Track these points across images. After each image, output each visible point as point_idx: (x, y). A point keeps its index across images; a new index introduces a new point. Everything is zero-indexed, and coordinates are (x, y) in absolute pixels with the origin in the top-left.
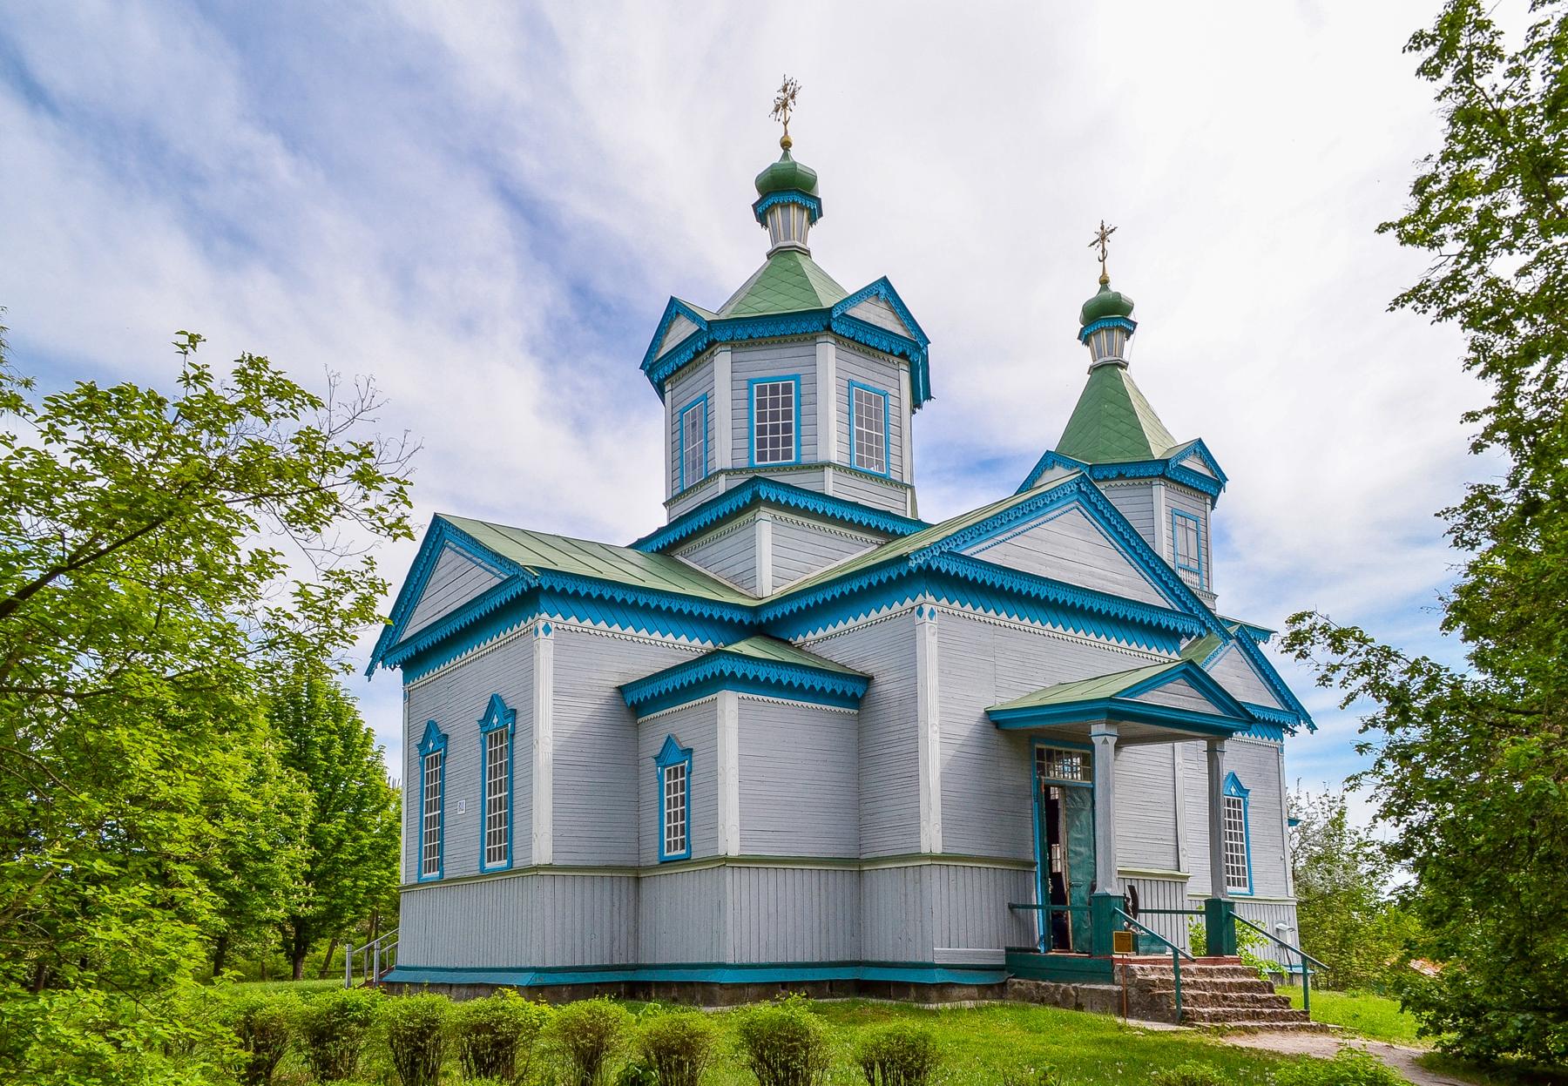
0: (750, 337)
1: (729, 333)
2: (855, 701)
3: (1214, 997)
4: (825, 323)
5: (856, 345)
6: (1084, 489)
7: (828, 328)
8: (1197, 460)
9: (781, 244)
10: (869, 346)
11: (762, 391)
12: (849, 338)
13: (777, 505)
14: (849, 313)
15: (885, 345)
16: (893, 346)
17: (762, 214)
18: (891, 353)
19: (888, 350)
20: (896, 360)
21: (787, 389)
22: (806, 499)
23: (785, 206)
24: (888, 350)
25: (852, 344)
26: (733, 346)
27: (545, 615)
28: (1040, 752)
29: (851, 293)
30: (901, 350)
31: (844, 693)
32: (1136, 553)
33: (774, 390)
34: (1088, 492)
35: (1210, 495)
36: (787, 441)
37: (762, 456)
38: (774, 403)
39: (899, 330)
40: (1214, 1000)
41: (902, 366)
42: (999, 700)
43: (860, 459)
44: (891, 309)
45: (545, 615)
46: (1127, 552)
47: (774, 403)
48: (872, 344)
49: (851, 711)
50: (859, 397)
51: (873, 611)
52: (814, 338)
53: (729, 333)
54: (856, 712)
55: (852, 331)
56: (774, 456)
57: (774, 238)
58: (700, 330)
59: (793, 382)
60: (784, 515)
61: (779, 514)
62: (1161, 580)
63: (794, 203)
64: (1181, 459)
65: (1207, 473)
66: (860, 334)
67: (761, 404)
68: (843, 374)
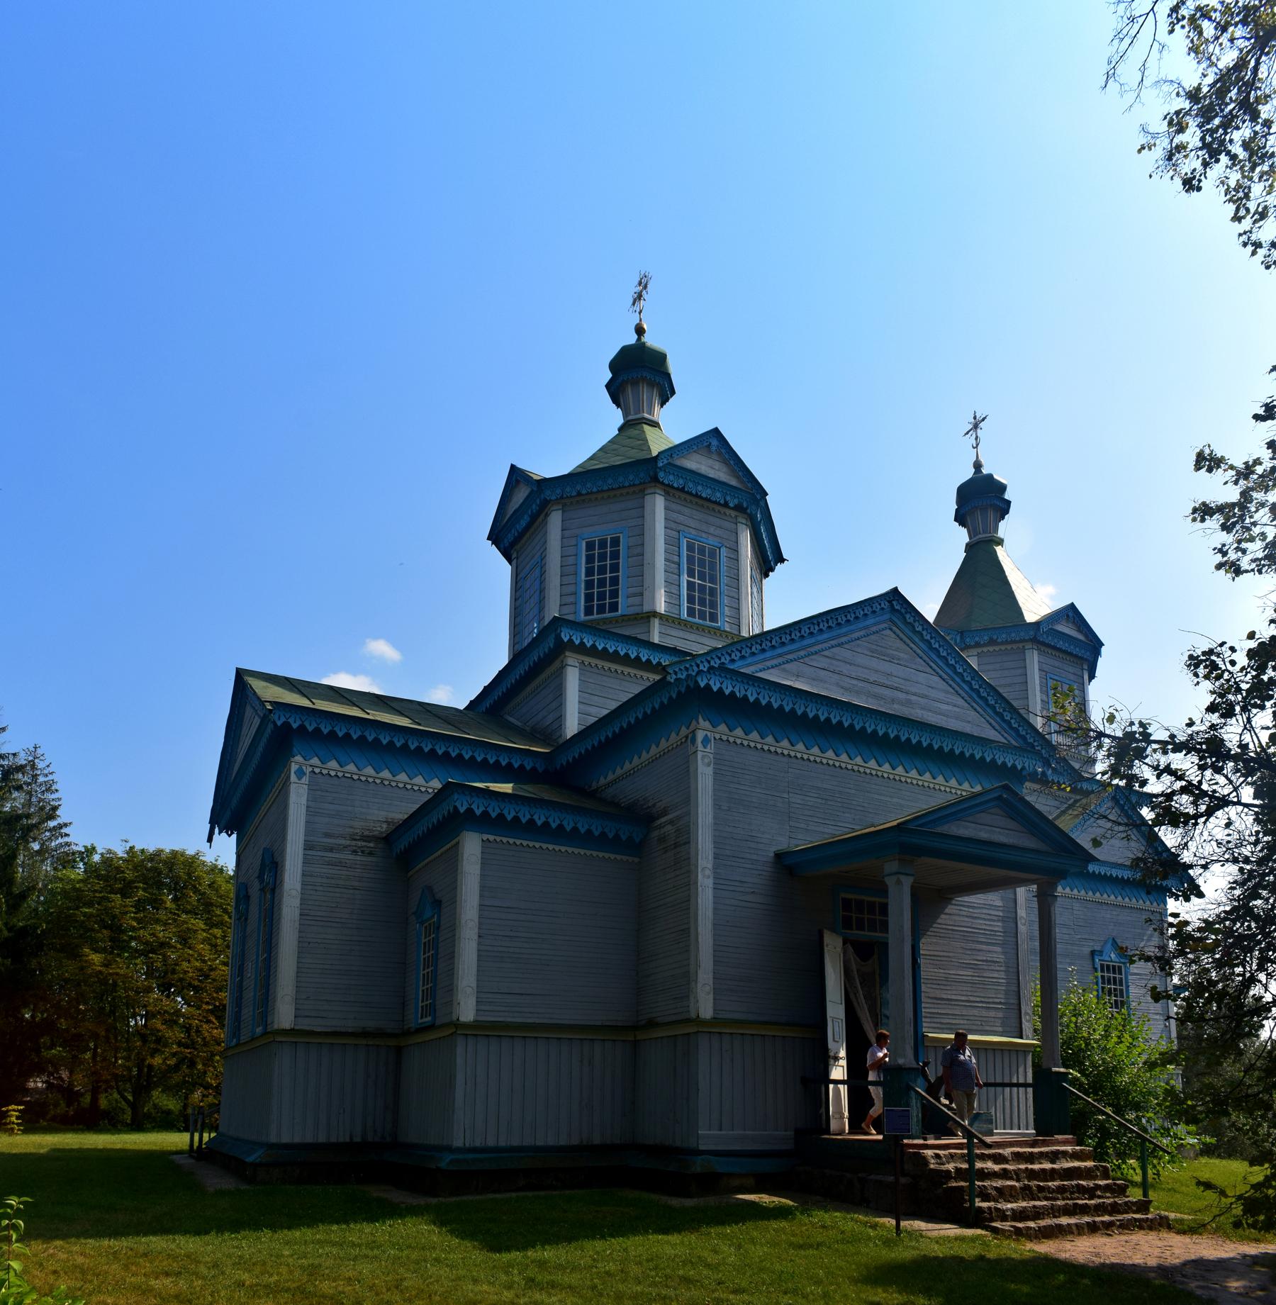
0: (579, 494)
1: (558, 491)
2: (636, 848)
3: (1026, 1188)
4: (652, 473)
5: (688, 497)
6: (897, 607)
7: (655, 480)
8: (1070, 625)
9: (630, 417)
10: (700, 497)
11: (590, 546)
12: (677, 489)
13: (581, 649)
14: (678, 463)
15: (718, 496)
16: (728, 498)
17: (616, 391)
18: (726, 505)
19: (722, 502)
20: (733, 513)
21: (616, 542)
22: (606, 641)
23: (635, 383)
24: (722, 502)
25: (683, 496)
26: (564, 505)
27: (298, 758)
28: (847, 904)
29: (677, 442)
30: (736, 501)
31: (617, 836)
32: (964, 681)
33: (603, 544)
34: (903, 611)
35: (1086, 660)
36: (615, 594)
37: (588, 611)
38: (602, 557)
39: (734, 482)
40: (1027, 1193)
41: (740, 519)
42: (793, 842)
43: (691, 612)
44: (725, 462)
45: (298, 758)
46: (953, 680)
47: (602, 557)
48: (704, 495)
49: (630, 859)
50: (690, 548)
51: (654, 746)
52: (642, 491)
53: (558, 491)
54: (637, 860)
55: (681, 481)
56: (601, 609)
57: (625, 414)
58: (532, 490)
59: (621, 535)
60: (594, 661)
61: (587, 660)
62: (1011, 727)
63: (644, 379)
64: (1052, 623)
65: (1081, 637)
66: (691, 485)
67: (590, 559)
68: (673, 525)
